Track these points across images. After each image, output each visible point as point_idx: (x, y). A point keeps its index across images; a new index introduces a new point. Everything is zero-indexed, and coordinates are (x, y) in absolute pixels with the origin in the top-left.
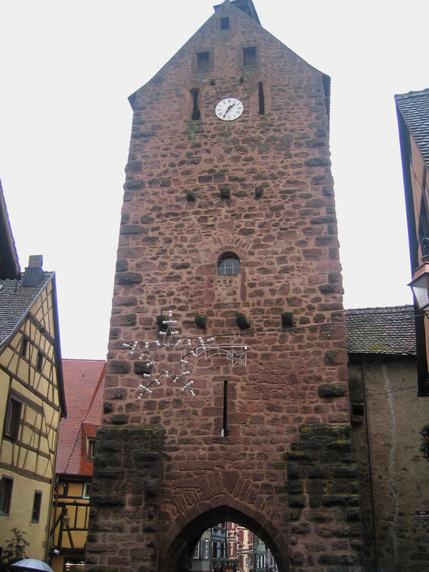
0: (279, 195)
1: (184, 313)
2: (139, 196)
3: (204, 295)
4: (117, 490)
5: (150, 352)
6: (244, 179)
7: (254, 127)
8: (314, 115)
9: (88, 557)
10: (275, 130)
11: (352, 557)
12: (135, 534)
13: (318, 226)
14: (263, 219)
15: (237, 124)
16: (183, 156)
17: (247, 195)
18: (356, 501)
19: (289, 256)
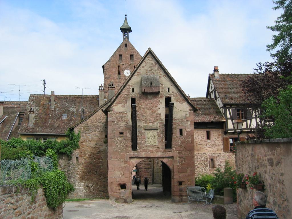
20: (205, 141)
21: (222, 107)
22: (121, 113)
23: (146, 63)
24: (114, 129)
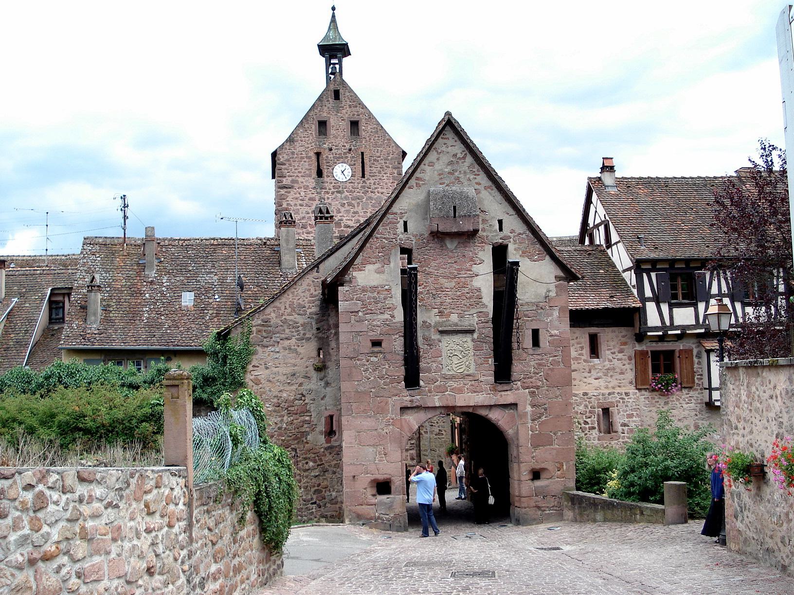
15: (348, 185)
20: (585, 361)
21: (629, 269)
22: (374, 288)
23: (439, 153)
24: (358, 333)
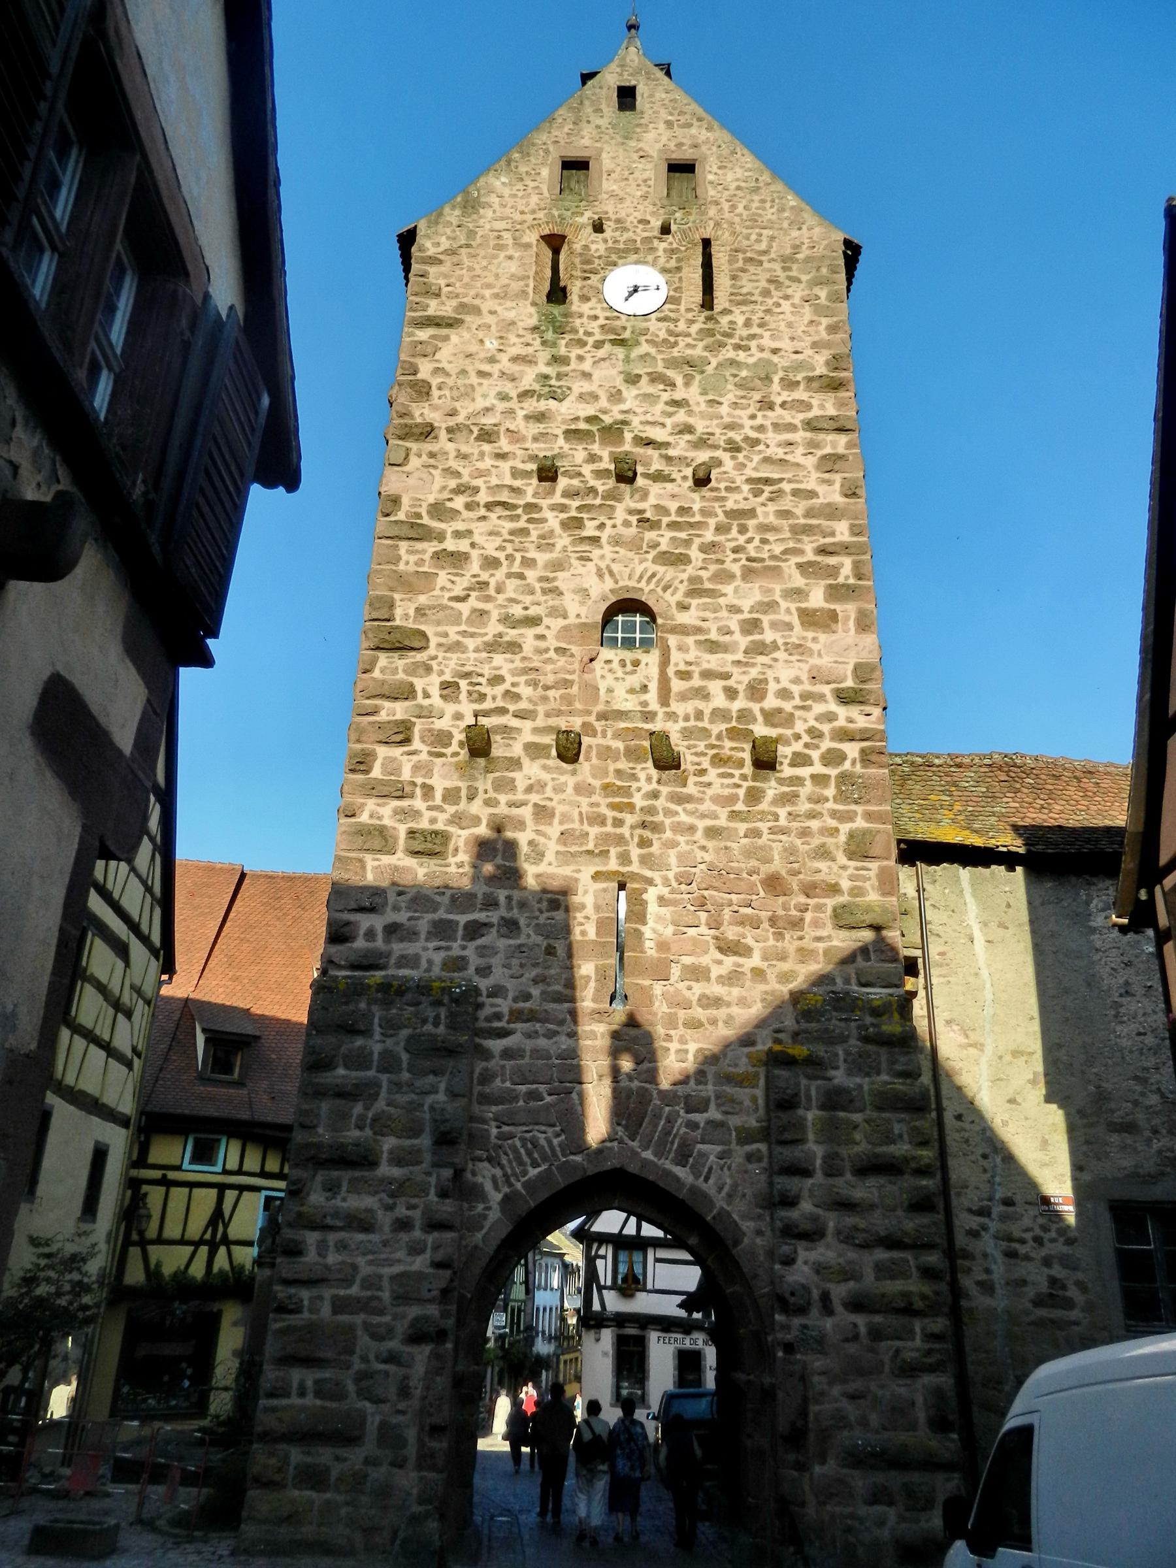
0: (746, 488)
1: (527, 725)
2: (424, 457)
3: (575, 688)
4: (361, 1128)
5: (446, 807)
6: (667, 445)
7: (688, 335)
8: (825, 322)
9: (280, 1295)
10: (738, 347)
11: (924, 1297)
12: (404, 1237)
13: (832, 560)
14: (709, 536)
16: (528, 379)
17: (673, 480)
18: (929, 1166)
19: (766, 620)
